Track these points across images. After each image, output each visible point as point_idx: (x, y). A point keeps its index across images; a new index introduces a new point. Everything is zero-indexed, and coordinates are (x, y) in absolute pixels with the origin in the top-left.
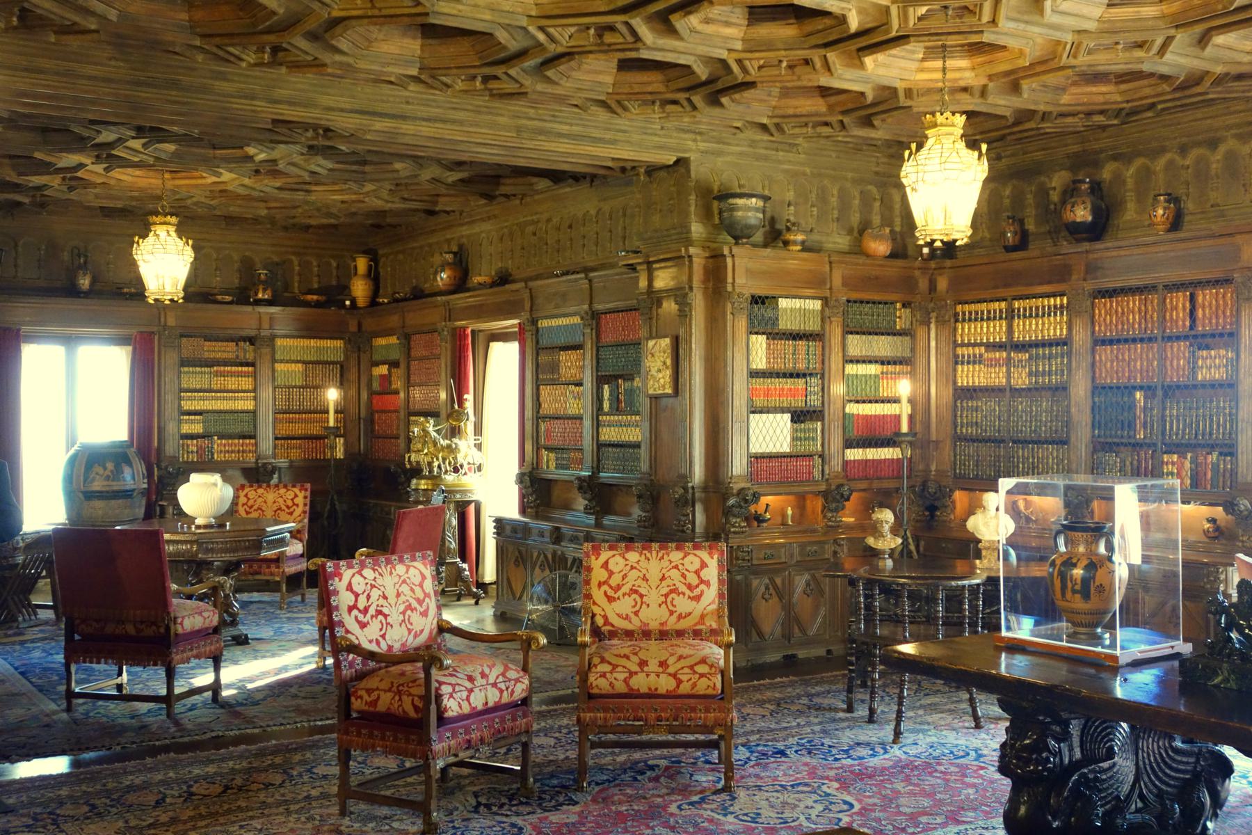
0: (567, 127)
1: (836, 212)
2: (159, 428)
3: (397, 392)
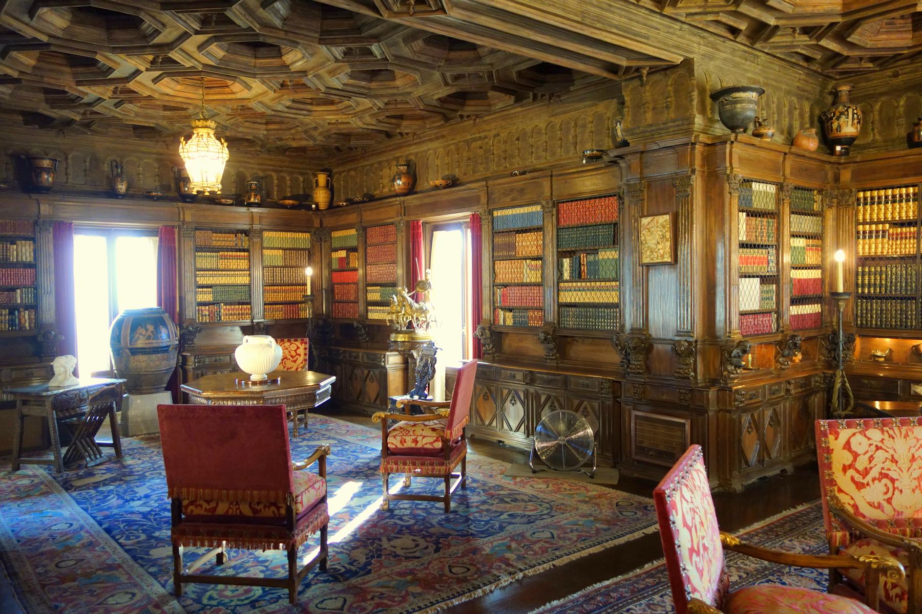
0: (617, 18)
1: (776, 116)
2: (181, 298)
3: (356, 270)
